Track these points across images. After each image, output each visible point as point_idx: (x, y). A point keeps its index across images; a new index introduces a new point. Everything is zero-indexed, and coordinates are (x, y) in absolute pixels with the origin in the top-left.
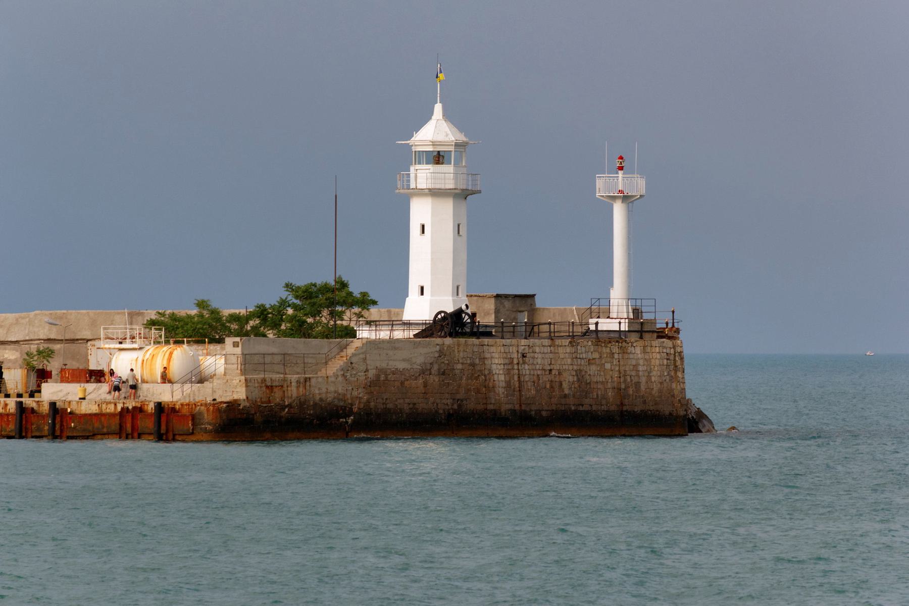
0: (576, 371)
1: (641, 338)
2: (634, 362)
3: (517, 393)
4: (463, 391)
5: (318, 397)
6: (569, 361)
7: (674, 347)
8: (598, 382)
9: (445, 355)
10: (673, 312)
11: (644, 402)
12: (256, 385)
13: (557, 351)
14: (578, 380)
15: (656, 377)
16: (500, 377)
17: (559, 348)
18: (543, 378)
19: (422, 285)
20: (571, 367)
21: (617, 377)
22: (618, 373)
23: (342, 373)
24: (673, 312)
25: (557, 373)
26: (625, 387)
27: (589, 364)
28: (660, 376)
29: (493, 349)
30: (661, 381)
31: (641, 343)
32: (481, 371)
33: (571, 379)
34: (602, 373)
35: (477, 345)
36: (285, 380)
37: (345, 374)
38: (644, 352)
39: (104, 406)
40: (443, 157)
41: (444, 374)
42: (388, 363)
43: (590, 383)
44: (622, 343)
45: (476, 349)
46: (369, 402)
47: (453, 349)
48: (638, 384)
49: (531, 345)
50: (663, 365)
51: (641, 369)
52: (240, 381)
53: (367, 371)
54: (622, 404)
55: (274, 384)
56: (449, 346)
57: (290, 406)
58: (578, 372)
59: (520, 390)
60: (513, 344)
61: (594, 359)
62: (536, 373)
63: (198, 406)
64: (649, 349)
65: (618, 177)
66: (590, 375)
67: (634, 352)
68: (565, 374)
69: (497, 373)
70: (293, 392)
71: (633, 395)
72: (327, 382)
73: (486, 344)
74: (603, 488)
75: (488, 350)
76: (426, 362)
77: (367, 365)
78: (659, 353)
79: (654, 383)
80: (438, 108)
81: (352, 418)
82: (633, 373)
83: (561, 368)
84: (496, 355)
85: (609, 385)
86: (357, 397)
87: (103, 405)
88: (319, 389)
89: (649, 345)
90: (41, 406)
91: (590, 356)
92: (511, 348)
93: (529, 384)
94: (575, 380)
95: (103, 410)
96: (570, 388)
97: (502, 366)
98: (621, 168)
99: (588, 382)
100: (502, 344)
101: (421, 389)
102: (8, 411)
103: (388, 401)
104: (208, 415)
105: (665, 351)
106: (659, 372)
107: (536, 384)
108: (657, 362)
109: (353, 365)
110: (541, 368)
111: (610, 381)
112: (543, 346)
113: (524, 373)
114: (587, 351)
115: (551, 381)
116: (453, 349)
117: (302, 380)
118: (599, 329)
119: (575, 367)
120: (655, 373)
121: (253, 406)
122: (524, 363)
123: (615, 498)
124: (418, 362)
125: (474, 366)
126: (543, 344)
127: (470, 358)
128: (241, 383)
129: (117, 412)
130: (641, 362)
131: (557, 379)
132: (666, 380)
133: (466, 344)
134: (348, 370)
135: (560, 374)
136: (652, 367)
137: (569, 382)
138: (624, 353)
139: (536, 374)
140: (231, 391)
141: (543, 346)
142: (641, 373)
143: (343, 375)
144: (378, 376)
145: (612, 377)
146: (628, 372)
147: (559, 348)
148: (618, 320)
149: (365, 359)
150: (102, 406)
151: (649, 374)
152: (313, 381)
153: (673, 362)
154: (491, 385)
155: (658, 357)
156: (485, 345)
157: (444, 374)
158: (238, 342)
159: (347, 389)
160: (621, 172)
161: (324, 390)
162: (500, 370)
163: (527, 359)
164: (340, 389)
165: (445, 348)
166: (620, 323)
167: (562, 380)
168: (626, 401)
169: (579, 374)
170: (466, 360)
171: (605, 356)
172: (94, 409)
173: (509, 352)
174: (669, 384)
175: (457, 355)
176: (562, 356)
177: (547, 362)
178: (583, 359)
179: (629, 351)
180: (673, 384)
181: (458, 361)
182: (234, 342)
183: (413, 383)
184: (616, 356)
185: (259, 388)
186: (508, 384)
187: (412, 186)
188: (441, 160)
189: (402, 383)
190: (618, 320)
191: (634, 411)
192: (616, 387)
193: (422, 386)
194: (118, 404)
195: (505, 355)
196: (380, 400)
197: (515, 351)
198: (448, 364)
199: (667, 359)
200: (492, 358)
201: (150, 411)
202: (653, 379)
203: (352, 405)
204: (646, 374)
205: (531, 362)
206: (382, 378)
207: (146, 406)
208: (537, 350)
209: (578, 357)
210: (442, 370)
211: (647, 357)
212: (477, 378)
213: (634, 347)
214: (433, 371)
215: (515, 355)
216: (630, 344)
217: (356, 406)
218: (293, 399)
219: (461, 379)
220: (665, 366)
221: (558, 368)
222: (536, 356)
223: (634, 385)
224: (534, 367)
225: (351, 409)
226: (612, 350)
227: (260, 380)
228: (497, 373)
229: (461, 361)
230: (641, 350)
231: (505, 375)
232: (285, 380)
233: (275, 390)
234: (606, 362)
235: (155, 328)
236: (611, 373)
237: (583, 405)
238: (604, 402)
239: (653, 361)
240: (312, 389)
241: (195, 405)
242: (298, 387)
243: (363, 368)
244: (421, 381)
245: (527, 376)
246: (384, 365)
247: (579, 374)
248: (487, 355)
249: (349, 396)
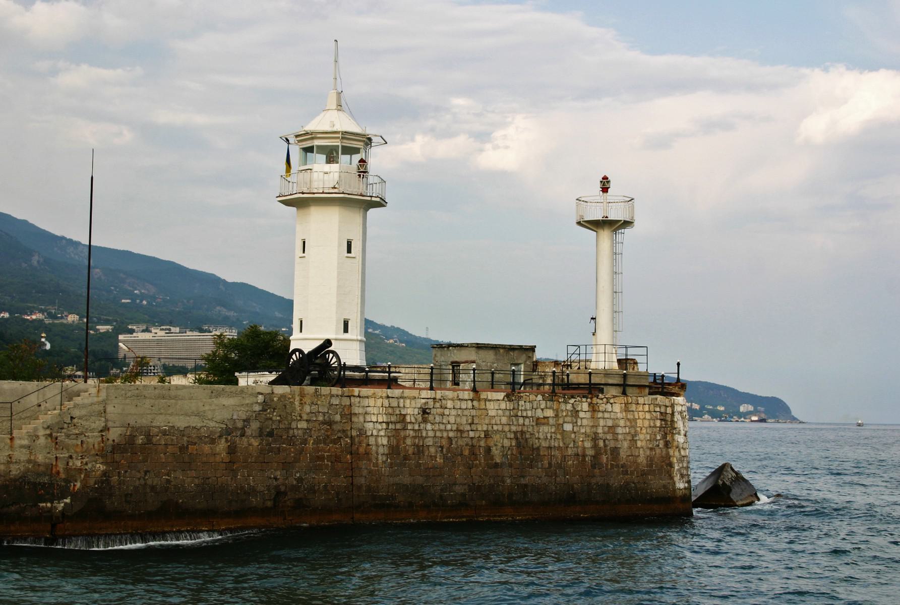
0: (515, 433)
2: (610, 423)
6: (504, 420)
8: (551, 448)
9: (274, 409)
10: (678, 364)
11: (626, 473)
13: (484, 407)
14: (519, 445)
15: (644, 442)
17: (487, 403)
18: (456, 442)
20: (507, 429)
23: (48, 432)
24: (678, 364)
25: (483, 436)
27: (537, 424)
28: (650, 440)
29: (371, 402)
30: (651, 446)
31: (622, 399)
33: (507, 443)
34: (559, 436)
35: (337, 396)
37: (54, 434)
38: (626, 409)
41: (271, 434)
43: (538, 449)
44: (591, 398)
45: (335, 401)
48: (615, 451)
50: (655, 427)
51: (620, 432)
53: (106, 429)
56: (283, 397)
58: (519, 435)
60: (405, 395)
61: (545, 418)
62: (445, 435)
64: (633, 407)
66: (539, 438)
67: (610, 410)
68: (496, 437)
69: (375, 433)
71: (607, 465)
72: (11, 447)
73: (356, 394)
74: (719, 532)
75: (359, 402)
76: (235, 417)
78: (649, 411)
79: (641, 449)
81: (68, 501)
82: (609, 437)
83: (490, 428)
85: (570, 452)
86: (81, 469)
89: (634, 402)
91: (539, 414)
92: (402, 401)
93: (432, 450)
94: (514, 444)
96: (504, 455)
97: (384, 426)
100: (384, 395)
105: (658, 409)
107: (444, 450)
108: (646, 423)
109: (75, 421)
112: (460, 399)
114: (535, 407)
115: (473, 446)
116: (291, 400)
118: (592, 382)
119: (514, 428)
122: (425, 421)
123: (625, 579)
124: (218, 417)
126: (461, 397)
127: (324, 414)
130: (622, 423)
132: (658, 446)
133: (316, 394)
134: (62, 428)
136: (639, 429)
137: (503, 447)
142: (620, 437)
143: (51, 435)
144: (131, 440)
147: (487, 403)
151: (633, 437)
153: (669, 423)
154: (362, 450)
155: (648, 416)
156: (354, 396)
159: (56, 457)
162: (379, 430)
163: (431, 418)
165: (275, 399)
167: (492, 444)
169: (521, 439)
170: (316, 416)
173: (399, 407)
176: (492, 413)
178: (527, 417)
181: (301, 417)
183: (207, 448)
186: (394, 450)
189: (183, 449)
192: (580, 454)
195: (390, 410)
198: (279, 421)
199: (661, 420)
202: (639, 444)
204: (629, 438)
205: (438, 419)
206: (140, 440)
208: (450, 404)
209: (519, 414)
211: (630, 416)
213: (611, 404)
214: (249, 432)
216: (605, 400)
219: (305, 442)
220: (658, 429)
221: (485, 429)
222: (447, 412)
223: (609, 452)
224: (442, 427)
226: (575, 406)
228: (375, 433)
229: (305, 417)
230: (621, 408)
231: (388, 437)
234: (564, 422)
236: (573, 436)
239: (639, 423)
243: (100, 424)
244: (222, 446)
246: (144, 422)
247: (521, 439)
249: (61, 466)
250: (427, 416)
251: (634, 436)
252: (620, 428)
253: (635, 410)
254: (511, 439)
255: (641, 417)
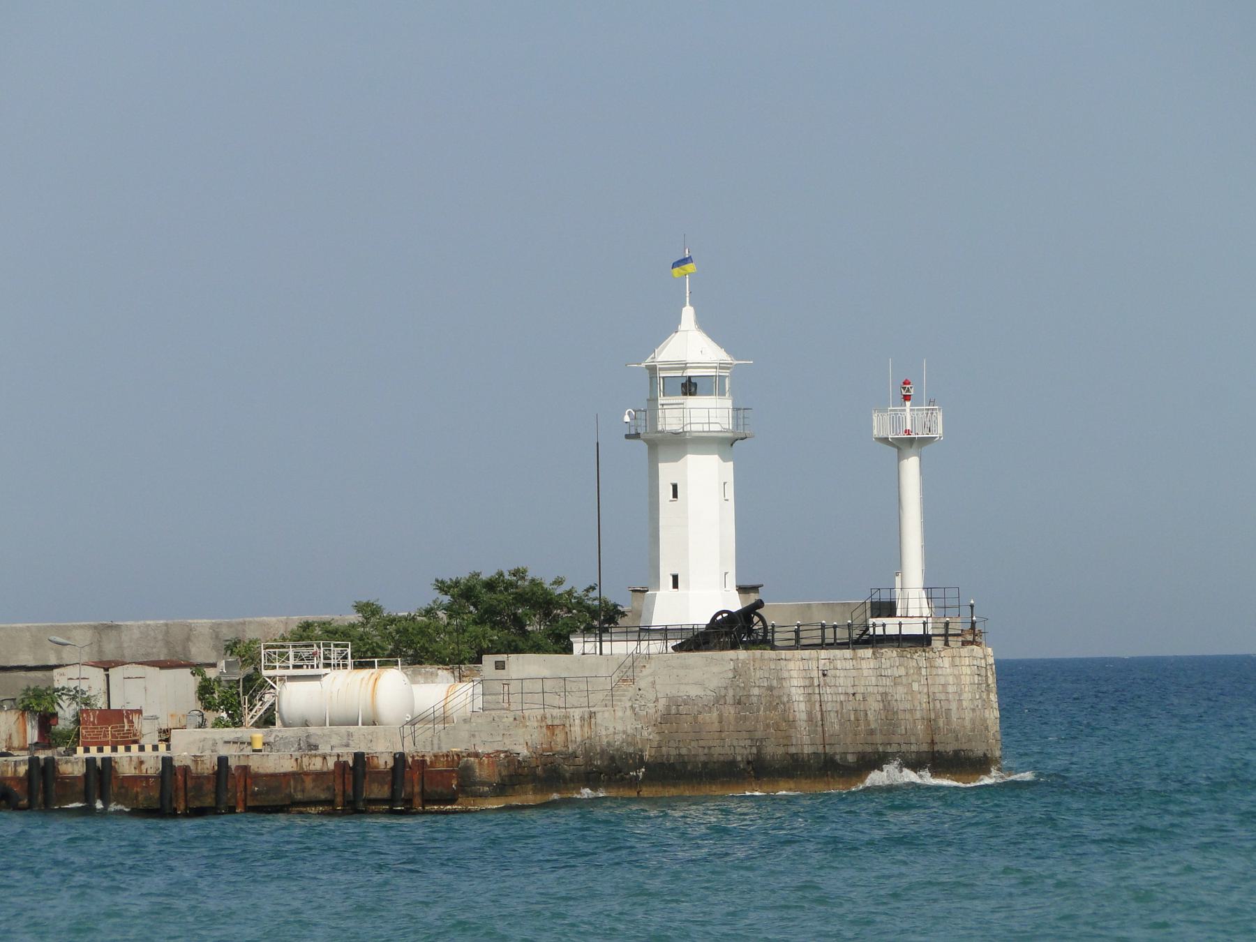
0: (882, 694)
1: (946, 644)
3: (820, 729)
4: (761, 727)
5: (605, 741)
7: (985, 658)
11: (957, 739)
12: (536, 724)
13: (859, 667)
16: (800, 709)
19: (675, 573)
21: (925, 703)
22: (926, 696)
26: (935, 716)
27: (895, 684)
29: (791, 665)
30: (972, 707)
31: (948, 652)
32: (779, 697)
36: (567, 717)
38: (953, 665)
39: (305, 760)
40: (695, 385)
42: (678, 689)
44: (928, 652)
46: (661, 747)
47: (748, 666)
49: (832, 658)
52: (515, 719)
53: (657, 700)
54: (933, 743)
55: (555, 723)
56: (744, 662)
57: (574, 755)
59: (822, 725)
60: (812, 656)
61: (900, 676)
63: (463, 757)
64: (957, 661)
65: (905, 410)
66: (896, 700)
68: (870, 700)
70: (577, 732)
77: (657, 691)
80: (688, 313)
82: (943, 697)
84: (794, 674)
86: (647, 739)
87: (304, 759)
88: (607, 729)
90: (200, 762)
92: (810, 662)
95: (304, 767)
98: (907, 398)
99: (895, 710)
101: (716, 726)
102: (144, 771)
103: (681, 745)
104: (480, 771)
106: (970, 694)
110: (844, 692)
111: (918, 708)
112: (845, 659)
113: (826, 699)
116: (748, 666)
117: (586, 716)
120: (966, 696)
121: (535, 756)
125: (771, 691)
126: (845, 657)
128: (518, 722)
129: (325, 769)
130: (951, 679)
131: (862, 707)
135: (864, 699)
136: (963, 686)
137: (875, 710)
138: (931, 667)
139: (838, 700)
140: (501, 735)
141: (845, 659)
144: (668, 707)
145: (920, 703)
146: (937, 695)
148: (922, 620)
149: (654, 683)
150: (302, 761)
152: (599, 716)
153: (984, 679)
154: (791, 718)
157: (739, 703)
158: (504, 662)
160: (908, 403)
161: (612, 730)
162: (800, 695)
164: (629, 727)
165: (740, 665)
166: (924, 623)
168: (937, 738)
171: (912, 671)
172: (288, 766)
174: (982, 711)
175: (753, 674)
176: (866, 673)
177: (850, 682)
179: (937, 665)
180: (986, 711)
182: (496, 662)
184: (924, 672)
185: (539, 728)
186: (810, 718)
187: (660, 428)
188: (693, 389)
190: (922, 620)
191: (945, 752)
193: (717, 721)
194: (328, 758)
196: (672, 744)
197: (815, 668)
198: (744, 688)
200: (791, 678)
201: (382, 766)
202: (965, 704)
203: (641, 751)
207: (376, 759)
208: (839, 664)
210: (738, 698)
211: (956, 672)
212: (775, 708)
215: (815, 674)
217: (647, 753)
218: (578, 743)
219: (758, 711)
221: (862, 691)
225: (641, 757)
227: (539, 718)
228: (797, 700)
232: (567, 717)
233: (557, 732)
234: (913, 681)
235: (334, 644)
237: (890, 744)
238: (913, 740)
240: (598, 728)
241: (458, 755)
242: (582, 727)
243: (652, 696)
244: (715, 714)
245: (829, 704)
248: (785, 675)
250: (826, 678)
251: (960, 695)
252: (950, 686)
253: (958, 664)
254: (879, 701)
255: (964, 673)
